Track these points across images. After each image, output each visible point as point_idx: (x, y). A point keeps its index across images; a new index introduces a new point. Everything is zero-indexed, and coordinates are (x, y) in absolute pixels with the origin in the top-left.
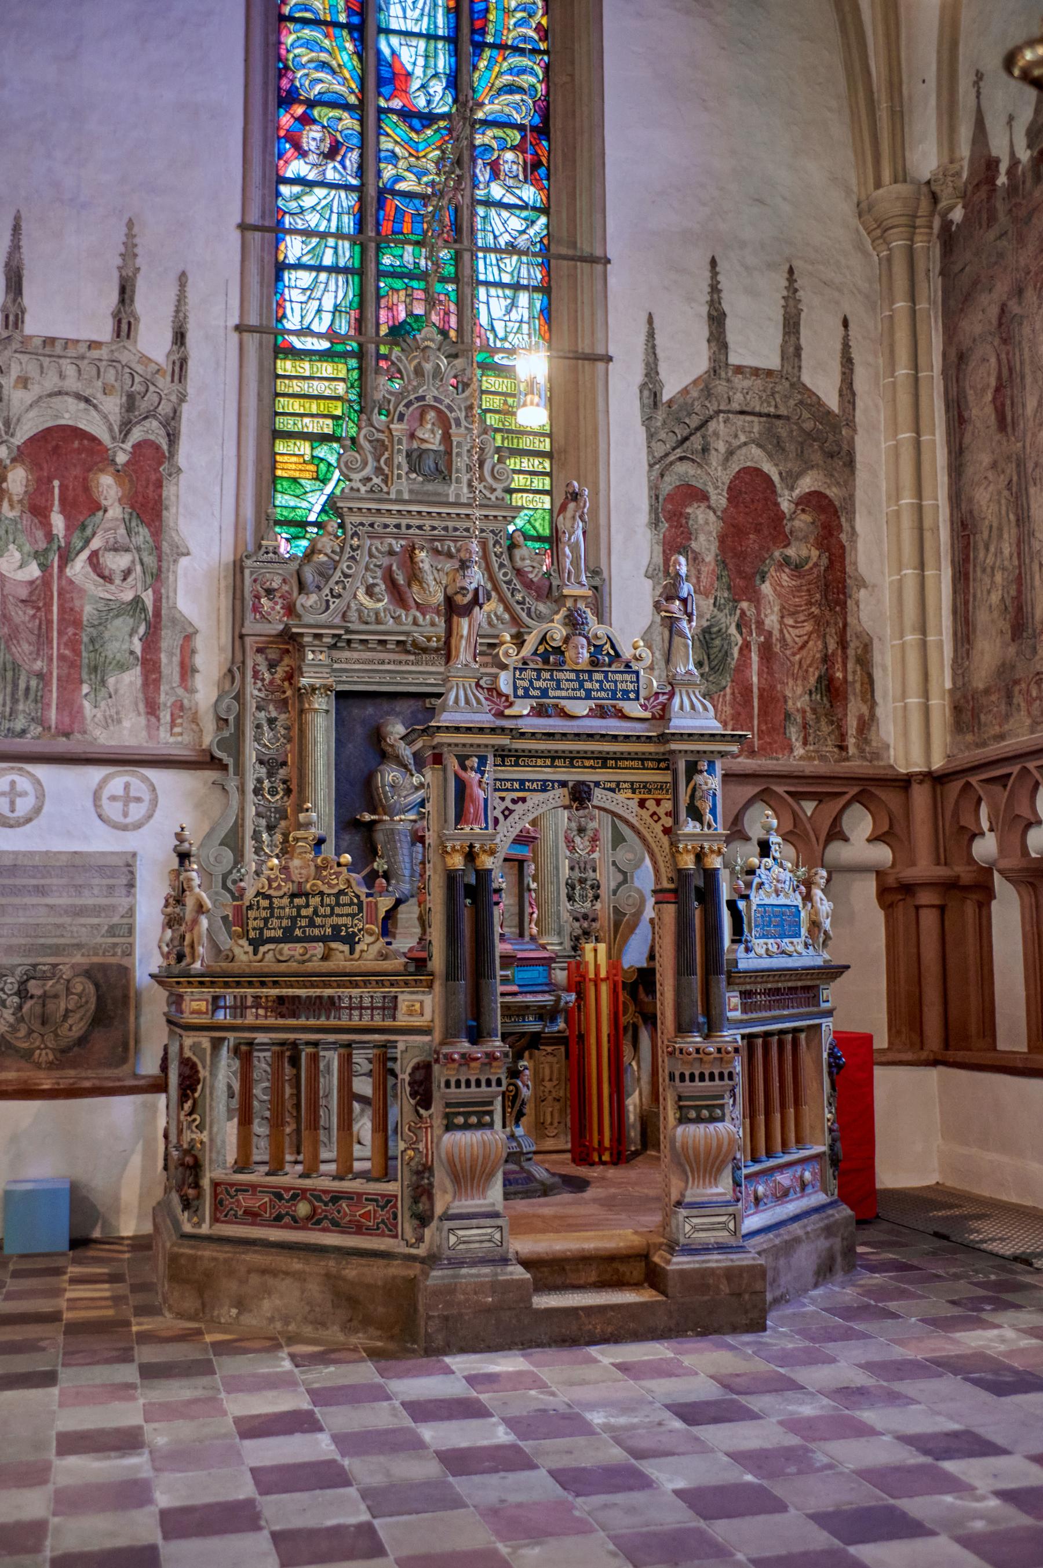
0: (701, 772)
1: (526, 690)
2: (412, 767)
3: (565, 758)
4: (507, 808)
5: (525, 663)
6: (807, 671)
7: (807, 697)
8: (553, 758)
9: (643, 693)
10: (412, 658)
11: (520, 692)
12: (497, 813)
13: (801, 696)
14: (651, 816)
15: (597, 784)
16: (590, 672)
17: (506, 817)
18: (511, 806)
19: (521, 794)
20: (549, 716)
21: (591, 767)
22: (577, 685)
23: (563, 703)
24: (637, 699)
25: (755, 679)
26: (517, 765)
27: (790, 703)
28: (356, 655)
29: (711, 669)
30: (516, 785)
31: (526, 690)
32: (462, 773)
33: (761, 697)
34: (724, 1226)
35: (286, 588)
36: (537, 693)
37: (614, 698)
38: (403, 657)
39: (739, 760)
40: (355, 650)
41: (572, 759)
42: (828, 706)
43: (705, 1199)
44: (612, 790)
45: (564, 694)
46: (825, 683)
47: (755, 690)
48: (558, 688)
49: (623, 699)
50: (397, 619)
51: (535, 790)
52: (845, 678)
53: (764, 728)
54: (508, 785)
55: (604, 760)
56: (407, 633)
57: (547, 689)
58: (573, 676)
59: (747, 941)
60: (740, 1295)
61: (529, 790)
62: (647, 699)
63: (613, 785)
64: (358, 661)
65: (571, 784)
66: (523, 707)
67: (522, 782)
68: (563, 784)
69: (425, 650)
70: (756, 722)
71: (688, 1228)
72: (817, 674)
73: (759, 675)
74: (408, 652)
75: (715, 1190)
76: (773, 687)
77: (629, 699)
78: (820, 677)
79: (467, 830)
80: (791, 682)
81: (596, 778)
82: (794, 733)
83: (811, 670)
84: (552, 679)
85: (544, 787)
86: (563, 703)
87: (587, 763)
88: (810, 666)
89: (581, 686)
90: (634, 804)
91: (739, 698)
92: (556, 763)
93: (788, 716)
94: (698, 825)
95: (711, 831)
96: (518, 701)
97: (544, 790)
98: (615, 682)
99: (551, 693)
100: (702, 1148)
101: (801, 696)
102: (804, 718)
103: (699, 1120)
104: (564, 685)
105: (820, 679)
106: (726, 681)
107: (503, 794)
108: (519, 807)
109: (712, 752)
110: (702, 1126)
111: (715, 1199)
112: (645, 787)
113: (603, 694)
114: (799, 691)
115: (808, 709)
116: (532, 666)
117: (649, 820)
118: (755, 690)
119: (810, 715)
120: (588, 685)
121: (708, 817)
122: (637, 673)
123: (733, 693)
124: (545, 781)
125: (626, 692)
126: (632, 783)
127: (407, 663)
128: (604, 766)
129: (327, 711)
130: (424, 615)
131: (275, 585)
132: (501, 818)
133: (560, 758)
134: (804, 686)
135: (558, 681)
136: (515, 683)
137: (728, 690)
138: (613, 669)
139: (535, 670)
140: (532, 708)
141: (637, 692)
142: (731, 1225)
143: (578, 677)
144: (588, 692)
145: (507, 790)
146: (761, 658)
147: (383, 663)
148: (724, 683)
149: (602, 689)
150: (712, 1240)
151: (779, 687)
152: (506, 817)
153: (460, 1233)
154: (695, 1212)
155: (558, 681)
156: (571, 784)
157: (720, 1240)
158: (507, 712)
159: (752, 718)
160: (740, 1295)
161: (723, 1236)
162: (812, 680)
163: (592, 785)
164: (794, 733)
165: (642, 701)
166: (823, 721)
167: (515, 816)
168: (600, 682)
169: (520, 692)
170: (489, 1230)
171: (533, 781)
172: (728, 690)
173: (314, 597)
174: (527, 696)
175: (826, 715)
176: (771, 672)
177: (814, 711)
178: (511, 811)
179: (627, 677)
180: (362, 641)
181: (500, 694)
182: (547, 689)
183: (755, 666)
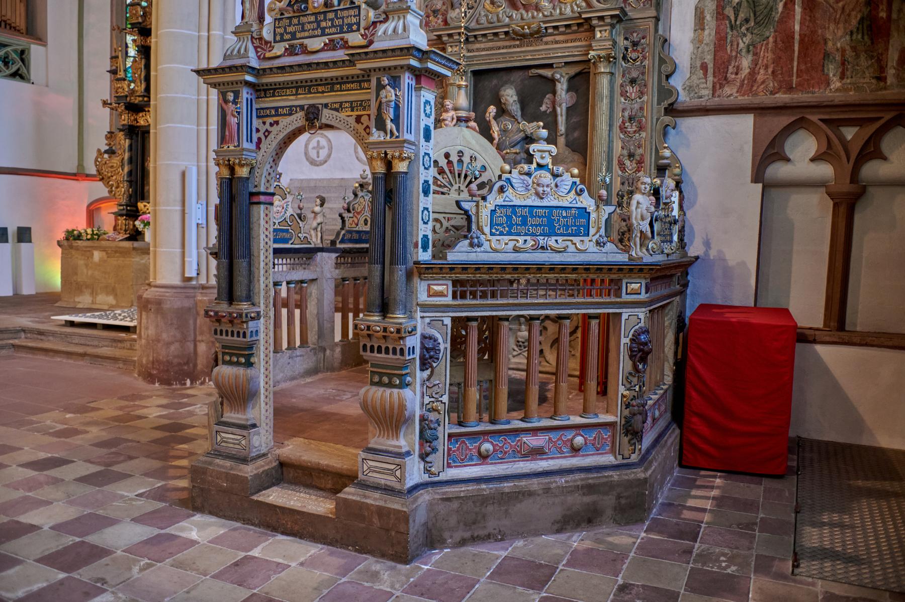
0: (384, 87)
1: (282, 35)
2: (520, 119)
3: (305, 87)
4: (267, 130)
5: (282, 14)
6: (849, 15)
7: (848, 38)
8: (297, 88)
9: (363, 24)
10: (518, 43)
11: (278, 38)
12: (261, 135)
13: (841, 37)
14: (365, 130)
15: (326, 106)
16: (325, 13)
17: (266, 137)
18: (270, 129)
19: (275, 119)
20: (297, 54)
21: (323, 92)
22: (315, 25)
23: (306, 41)
24: (358, 30)
25: (797, 27)
26: (274, 96)
27: (830, 44)
28: (482, 46)
29: (756, 23)
30: (273, 112)
31: (282, 35)
32: (224, 105)
33: (802, 41)
34: (392, 473)
35: (444, 7)
36: (287, 37)
37: (342, 32)
38: (513, 43)
39: (777, 95)
40: (481, 42)
41: (308, 86)
42: (869, 43)
43: (384, 448)
44: (336, 110)
45: (306, 34)
46: (866, 23)
47: (797, 37)
48: (303, 30)
49: (348, 32)
50: (510, 17)
51: (285, 115)
52: (889, 17)
53: (803, 67)
54: (268, 112)
55: (331, 84)
56: (508, 26)
57: (295, 32)
58: (312, 18)
59: (472, 238)
60: (388, 530)
61: (281, 115)
62: (367, 28)
63: (337, 106)
64: (484, 50)
65: (306, 107)
66: (279, 49)
67: (276, 109)
68: (302, 107)
69: (524, 36)
70: (795, 64)
71: (365, 468)
72: (859, 16)
73: (802, 24)
74: (514, 39)
75: (394, 442)
76: (814, 32)
77: (353, 31)
78: (862, 19)
79: (226, 148)
80: (832, 26)
81: (324, 101)
82: (832, 70)
83: (854, 13)
84: (299, 24)
85: (291, 111)
86: (306, 41)
87: (320, 89)
88: (853, 10)
89: (319, 26)
90: (352, 120)
91: (780, 45)
92: (300, 92)
93: (826, 55)
94: (382, 134)
95: (393, 139)
96: (276, 45)
97: (290, 114)
98: (342, 18)
99: (298, 35)
100: (387, 407)
101: (841, 37)
102: (843, 56)
103: (380, 384)
104: (307, 27)
105: (861, 21)
106: (770, 33)
107: (265, 119)
108: (274, 129)
109: (395, 67)
110: (382, 389)
111: (391, 449)
112: (361, 105)
113: (333, 30)
114: (840, 33)
115: (848, 48)
116: (287, 15)
117: (363, 133)
118: (797, 37)
119: (849, 53)
120: (323, 24)
121: (389, 125)
122: (359, 7)
123: (775, 42)
124: (291, 107)
125: (350, 25)
126: (351, 102)
127: (514, 46)
128: (332, 90)
129: (467, 86)
130: (527, 11)
131: (438, 7)
132: (263, 138)
133: (301, 87)
134: (845, 28)
135: (303, 25)
136: (275, 31)
137: (771, 39)
138: (341, 7)
139: (288, 18)
140: (286, 49)
141: (358, 24)
142: (398, 473)
143: (316, 18)
144: (323, 29)
145: (267, 116)
146: (804, 9)
147: (499, 48)
148: (767, 34)
149: (333, 26)
150: (383, 482)
151: (820, 31)
152: (266, 137)
153: (223, 435)
154: (370, 456)
155: (303, 25)
156: (306, 107)
157: (388, 483)
158: (268, 55)
159: (792, 60)
160: (388, 530)
161: (390, 481)
162: (854, 22)
163: (320, 106)
164: (832, 70)
165: (362, 31)
166: (863, 57)
167: (272, 136)
168: (332, 20)
169: (278, 38)
170: (239, 437)
171: (283, 107)
172: (771, 39)
173: (457, 10)
174: (282, 40)
175: (866, 52)
176: (813, 19)
177: (854, 49)
178: (269, 132)
179: (352, 12)
180: (484, 35)
181: (267, 42)
182: (295, 32)
183: (798, 17)
